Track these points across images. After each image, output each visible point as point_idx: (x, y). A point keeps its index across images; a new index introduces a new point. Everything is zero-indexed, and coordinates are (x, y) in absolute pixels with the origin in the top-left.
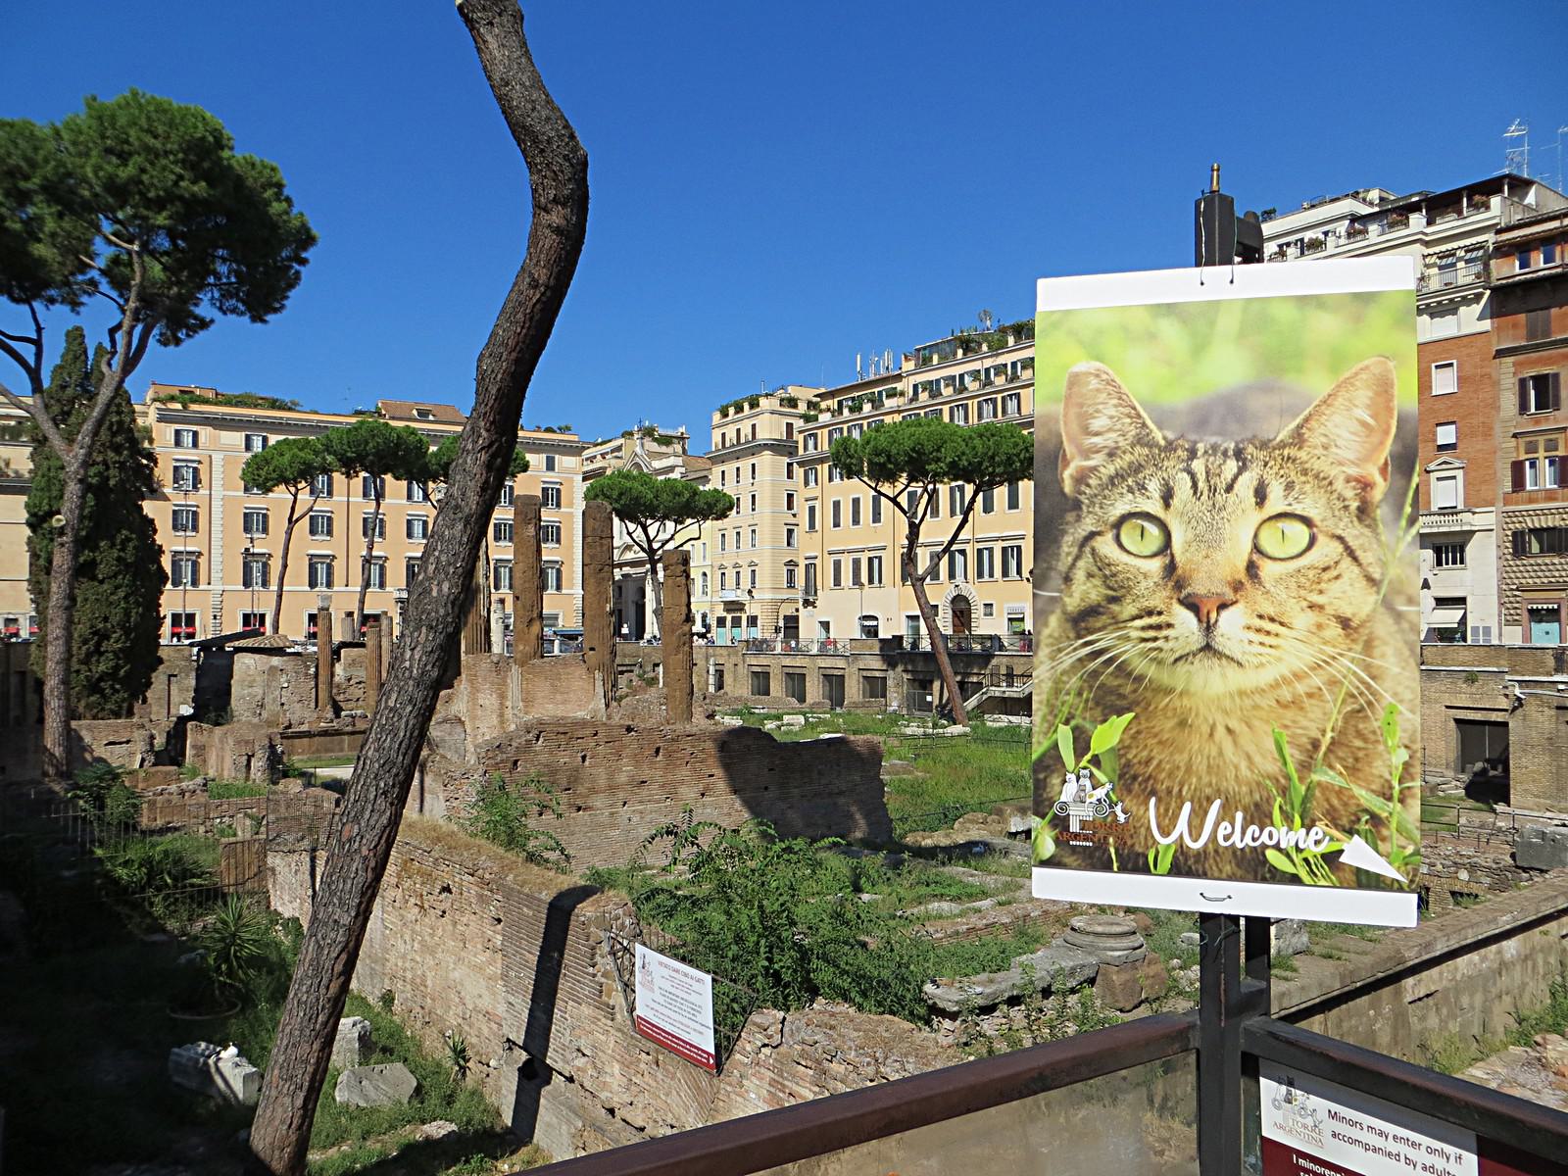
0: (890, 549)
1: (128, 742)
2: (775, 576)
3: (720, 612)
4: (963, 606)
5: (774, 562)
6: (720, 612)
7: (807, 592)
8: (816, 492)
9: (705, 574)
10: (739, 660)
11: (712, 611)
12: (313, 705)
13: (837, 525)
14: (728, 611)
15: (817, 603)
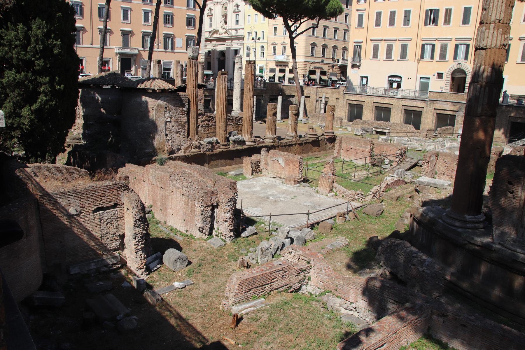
0: (414, 41)
1: (115, 206)
2: (306, 50)
3: (273, 66)
4: (458, 75)
5: (306, 42)
6: (273, 66)
7: (354, 59)
8: (366, 6)
9: (263, 47)
10: (341, 96)
11: (266, 65)
12: (186, 135)
13: (378, 24)
14: (277, 65)
15: (361, 67)
